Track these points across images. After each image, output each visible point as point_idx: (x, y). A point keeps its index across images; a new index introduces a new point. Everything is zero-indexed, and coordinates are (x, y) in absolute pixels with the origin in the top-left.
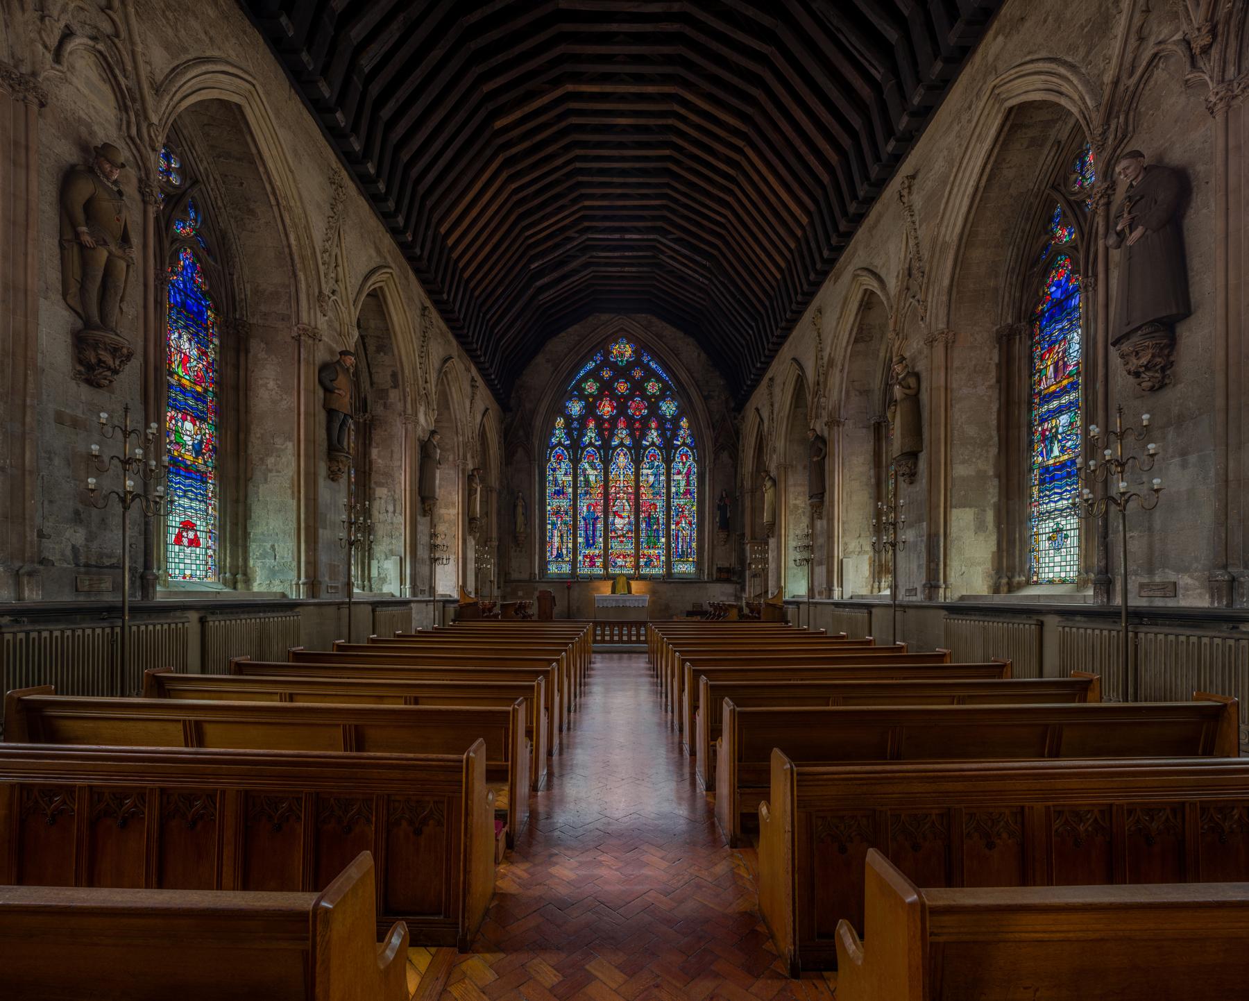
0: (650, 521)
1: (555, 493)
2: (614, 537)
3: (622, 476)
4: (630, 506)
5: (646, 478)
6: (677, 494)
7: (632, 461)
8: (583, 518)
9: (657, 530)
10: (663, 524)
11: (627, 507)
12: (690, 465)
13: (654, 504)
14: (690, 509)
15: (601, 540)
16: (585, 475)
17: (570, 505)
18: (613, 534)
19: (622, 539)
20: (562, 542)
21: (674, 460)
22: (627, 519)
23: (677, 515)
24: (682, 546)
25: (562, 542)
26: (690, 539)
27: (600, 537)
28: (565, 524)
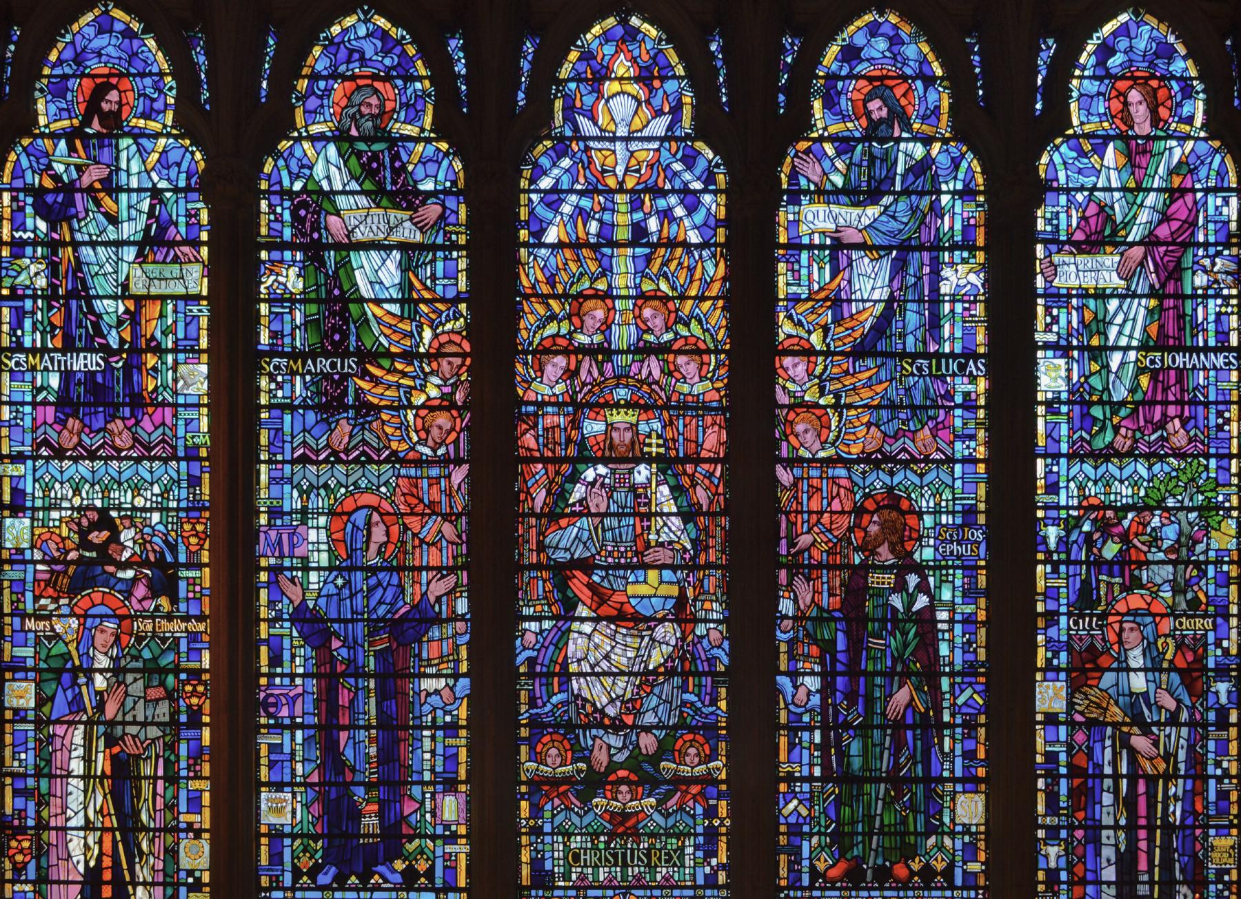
0: (856, 644)
1: (66, 403)
2: (554, 782)
3: (624, 264)
4: (688, 515)
5: (821, 275)
6: (1087, 420)
7: (701, 131)
8: (304, 618)
9: (930, 726)
10: (970, 670)
11: (673, 529)
12: (1186, 167)
13: (892, 501)
14: (1187, 542)
15: (451, 808)
16: (314, 251)
17: (194, 508)
18: (555, 763)
19: (624, 800)
20: (129, 826)
21: (1056, 122)
22: (668, 632)
23: (1085, 600)
24: (1126, 862)
25: (129, 826)
26: (1189, 797)
27: (450, 785)
28: (152, 671)
